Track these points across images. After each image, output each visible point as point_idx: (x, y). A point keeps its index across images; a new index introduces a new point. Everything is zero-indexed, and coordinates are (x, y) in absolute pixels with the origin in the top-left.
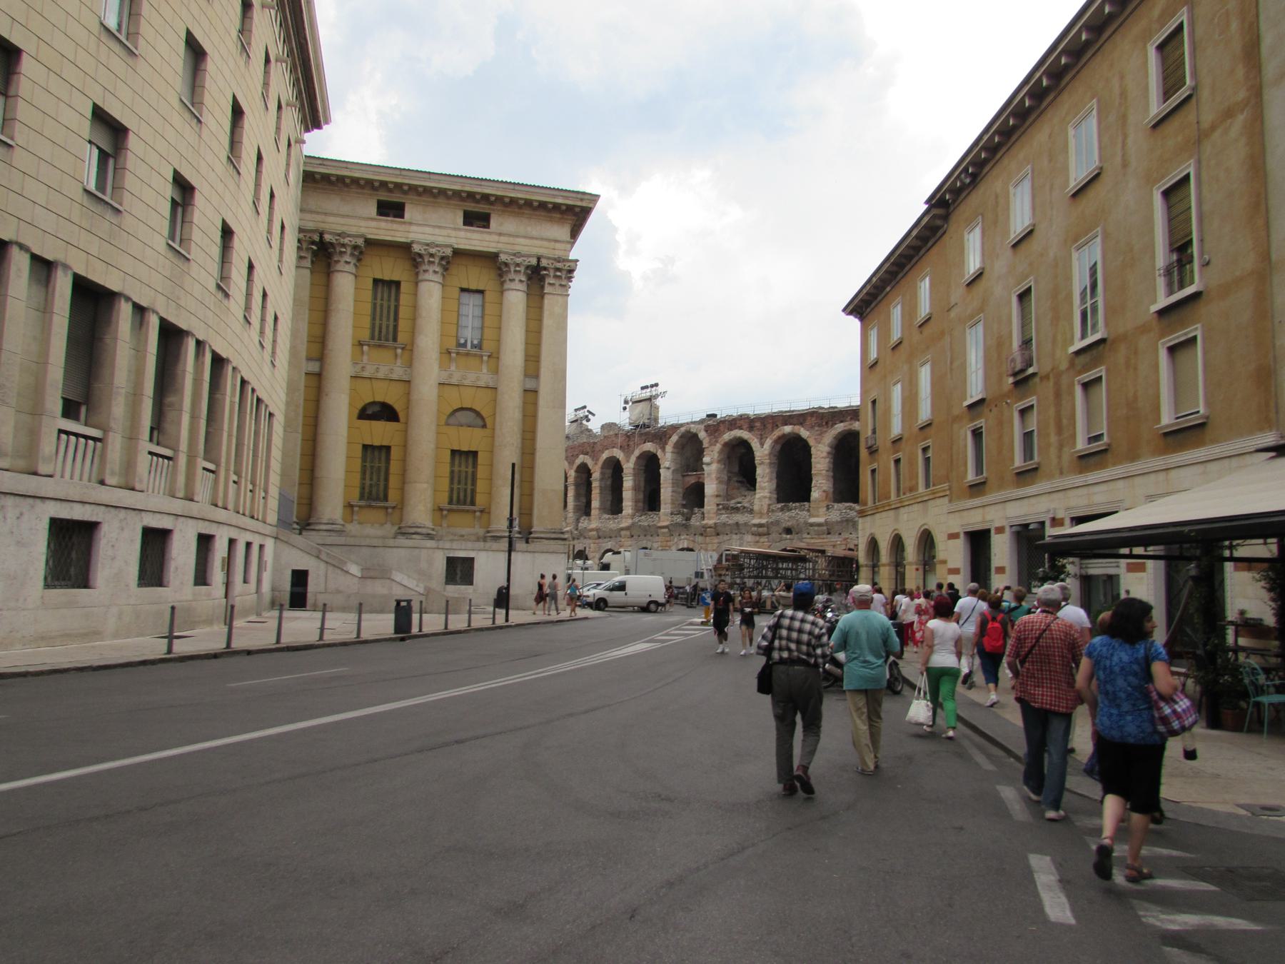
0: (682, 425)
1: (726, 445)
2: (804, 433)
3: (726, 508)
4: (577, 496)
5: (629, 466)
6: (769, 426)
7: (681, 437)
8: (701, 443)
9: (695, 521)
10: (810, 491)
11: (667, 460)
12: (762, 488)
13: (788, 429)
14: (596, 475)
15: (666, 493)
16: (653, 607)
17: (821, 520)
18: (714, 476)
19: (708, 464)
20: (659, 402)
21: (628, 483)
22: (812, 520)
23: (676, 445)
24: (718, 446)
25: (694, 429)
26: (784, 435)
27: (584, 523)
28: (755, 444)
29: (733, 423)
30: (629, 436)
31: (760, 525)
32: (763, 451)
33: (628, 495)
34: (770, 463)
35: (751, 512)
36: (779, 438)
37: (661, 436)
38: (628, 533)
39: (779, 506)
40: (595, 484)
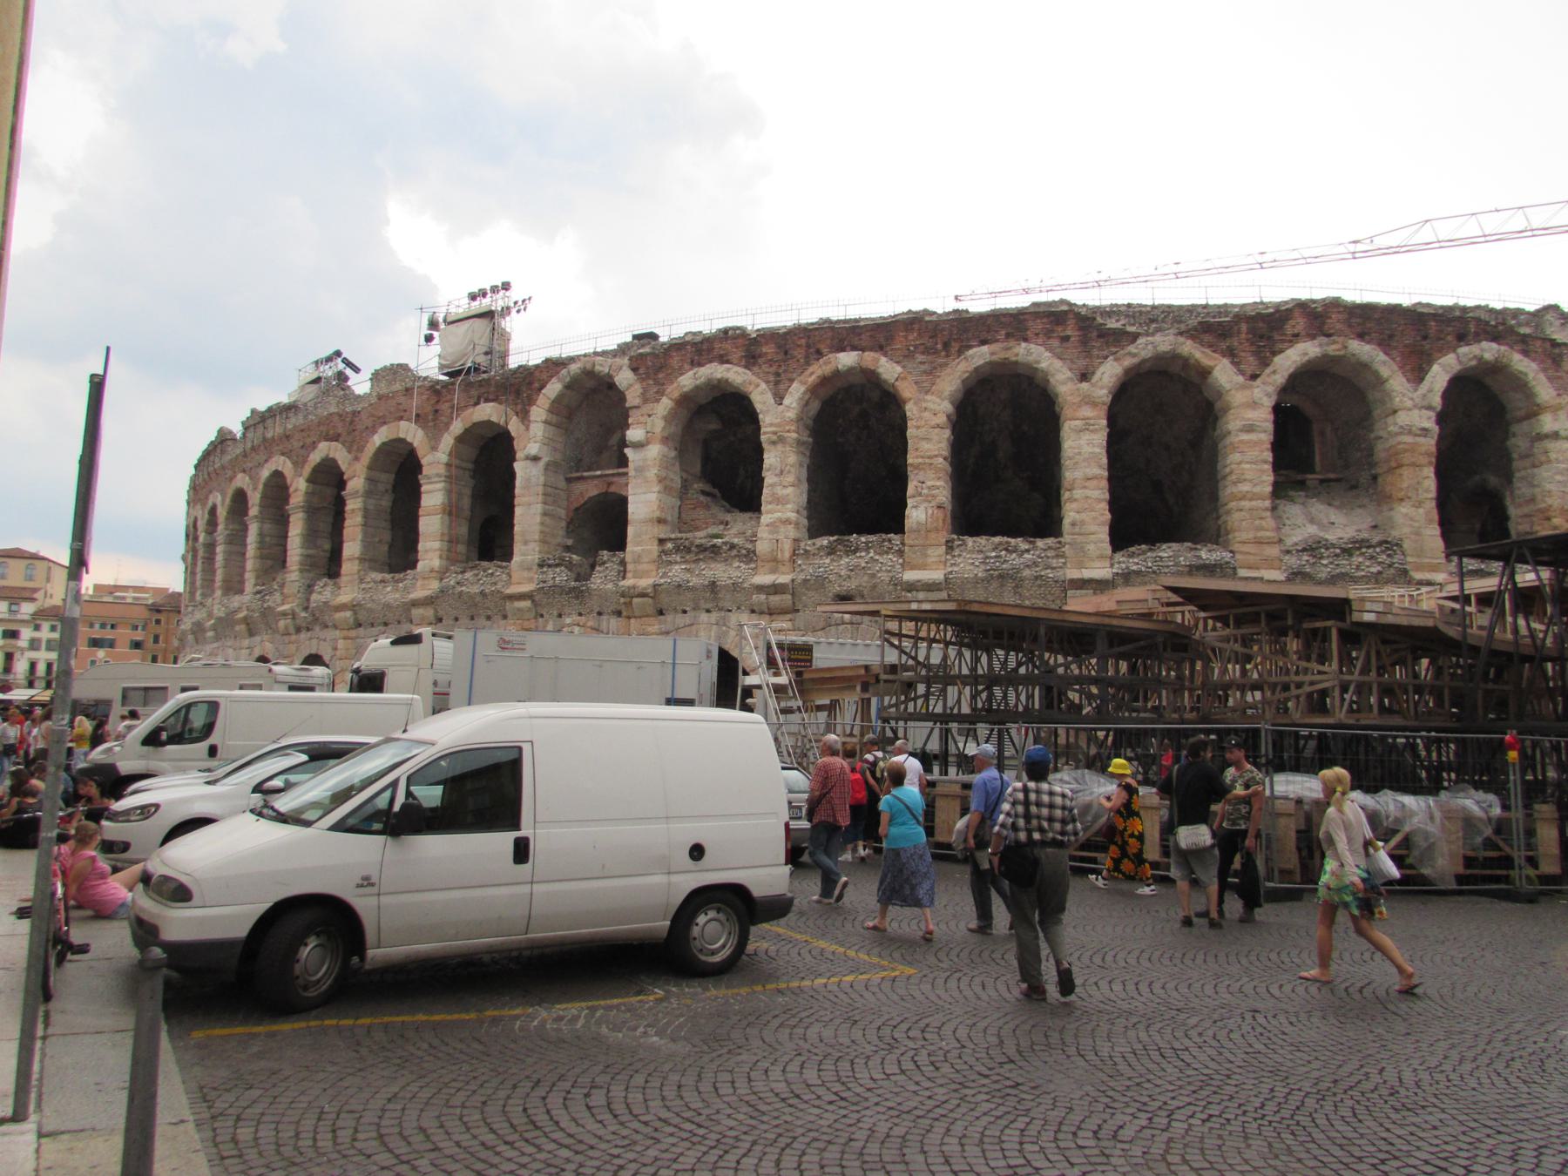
0: (572, 359)
1: (684, 400)
2: (888, 369)
3: (683, 549)
4: (311, 536)
5: (436, 460)
6: (799, 354)
7: (568, 387)
8: (622, 397)
9: (601, 581)
10: (903, 505)
11: (533, 440)
12: (778, 500)
13: (847, 359)
14: (356, 483)
15: (530, 515)
16: (712, 934)
17: (937, 575)
18: (652, 473)
19: (638, 446)
20: (511, 324)
21: (433, 496)
22: (910, 576)
23: (556, 406)
24: (665, 405)
25: (602, 367)
26: (837, 374)
27: (324, 593)
28: (761, 397)
29: (700, 348)
30: (436, 391)
31: (776, 589)
32: (781, 413)
33: (431, 525)
34: (799, 443)
35: (750, 556)
36: (824, 381)
37: (521, 386)
38: (429, 612)
39: (824, 541)
40: (353, 505)
